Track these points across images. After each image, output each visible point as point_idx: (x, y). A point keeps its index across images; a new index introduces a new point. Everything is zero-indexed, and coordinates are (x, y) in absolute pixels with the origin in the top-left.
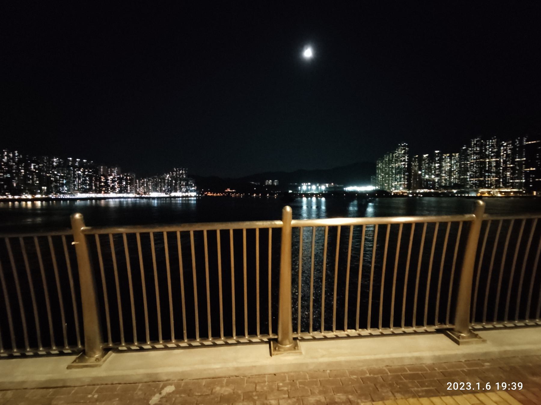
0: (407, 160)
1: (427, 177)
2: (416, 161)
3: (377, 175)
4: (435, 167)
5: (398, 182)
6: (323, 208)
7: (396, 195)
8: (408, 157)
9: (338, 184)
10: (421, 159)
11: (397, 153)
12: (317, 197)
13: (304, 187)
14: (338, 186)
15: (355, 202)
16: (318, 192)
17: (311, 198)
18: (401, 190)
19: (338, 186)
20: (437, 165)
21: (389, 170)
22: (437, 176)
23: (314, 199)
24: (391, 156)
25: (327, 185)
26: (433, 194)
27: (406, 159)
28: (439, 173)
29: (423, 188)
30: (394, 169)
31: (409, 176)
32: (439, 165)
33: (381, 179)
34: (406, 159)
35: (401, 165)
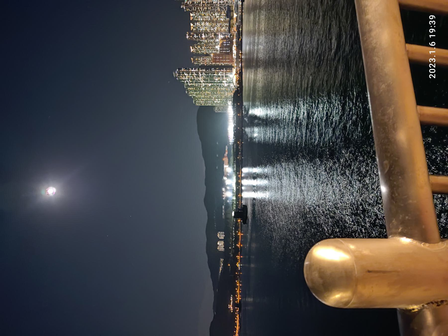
0: (197, 70)
1: (218, 47)
2: (198, 60)
3: (214, 105)
4: (206, 39)
5: (223, 80)
6: (257, 170)
7: (240, 81)
8: (192, 69)
9: (225, 153)
10: (198, 55)
11: (188, 81)
12: (242, 178)
13: (229, 195)
14: (227, 153)
15: (248, 130)
16: (235, 177)
17: (242, 185)
18: (233, 76)
19: (227, 153)
20: (203, 36)
21: (208, 90)
22: (216, 35)
23: (245, 182)
24: (190, 89)
25: (225, 166)
26: (239, 40)
27: (195, 70)
28: (213, 34)
29: (231, 50)
30: (207, 84)
31: (215, 67)
32: (203, 35)
33: (219, 100)
34: (195, 70)
35: (203, 76)
